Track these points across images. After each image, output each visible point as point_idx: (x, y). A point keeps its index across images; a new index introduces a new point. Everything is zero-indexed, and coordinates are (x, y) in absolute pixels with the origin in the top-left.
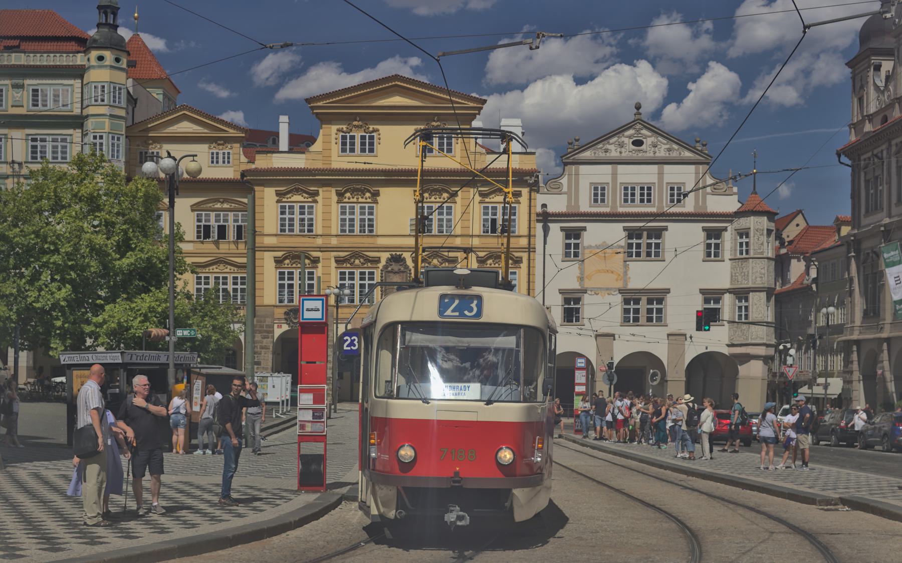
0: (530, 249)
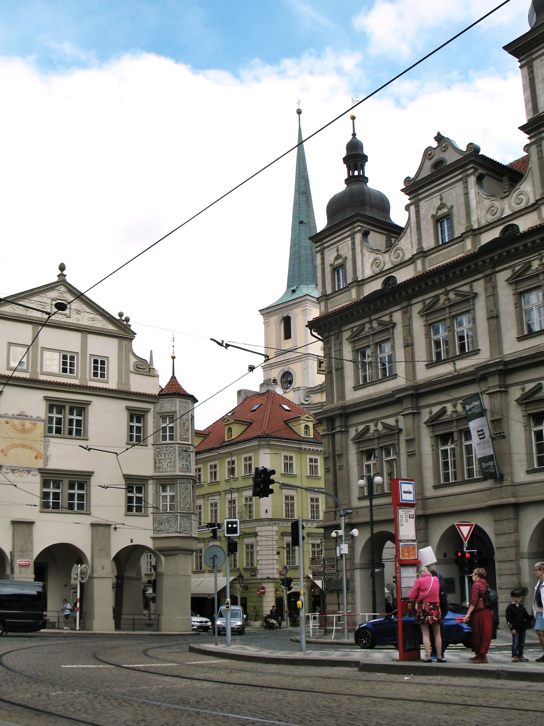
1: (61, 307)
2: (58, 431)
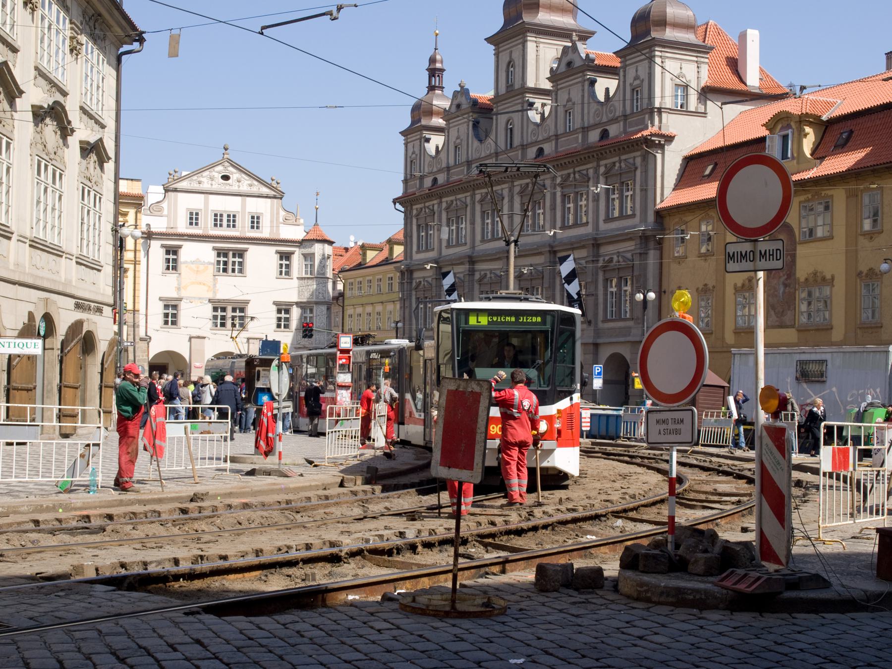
0: (135, 262)
1: (226, 178)
2: (225, 270)
